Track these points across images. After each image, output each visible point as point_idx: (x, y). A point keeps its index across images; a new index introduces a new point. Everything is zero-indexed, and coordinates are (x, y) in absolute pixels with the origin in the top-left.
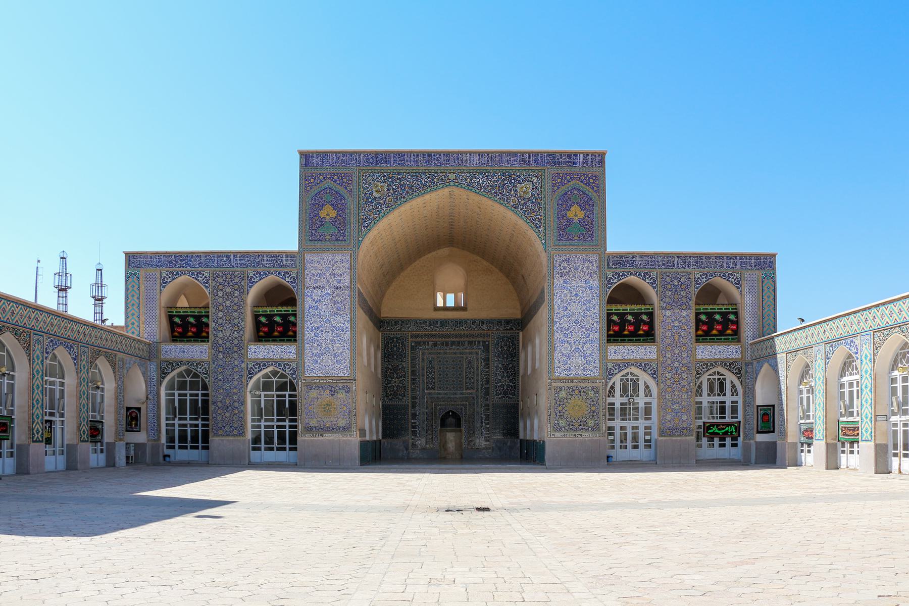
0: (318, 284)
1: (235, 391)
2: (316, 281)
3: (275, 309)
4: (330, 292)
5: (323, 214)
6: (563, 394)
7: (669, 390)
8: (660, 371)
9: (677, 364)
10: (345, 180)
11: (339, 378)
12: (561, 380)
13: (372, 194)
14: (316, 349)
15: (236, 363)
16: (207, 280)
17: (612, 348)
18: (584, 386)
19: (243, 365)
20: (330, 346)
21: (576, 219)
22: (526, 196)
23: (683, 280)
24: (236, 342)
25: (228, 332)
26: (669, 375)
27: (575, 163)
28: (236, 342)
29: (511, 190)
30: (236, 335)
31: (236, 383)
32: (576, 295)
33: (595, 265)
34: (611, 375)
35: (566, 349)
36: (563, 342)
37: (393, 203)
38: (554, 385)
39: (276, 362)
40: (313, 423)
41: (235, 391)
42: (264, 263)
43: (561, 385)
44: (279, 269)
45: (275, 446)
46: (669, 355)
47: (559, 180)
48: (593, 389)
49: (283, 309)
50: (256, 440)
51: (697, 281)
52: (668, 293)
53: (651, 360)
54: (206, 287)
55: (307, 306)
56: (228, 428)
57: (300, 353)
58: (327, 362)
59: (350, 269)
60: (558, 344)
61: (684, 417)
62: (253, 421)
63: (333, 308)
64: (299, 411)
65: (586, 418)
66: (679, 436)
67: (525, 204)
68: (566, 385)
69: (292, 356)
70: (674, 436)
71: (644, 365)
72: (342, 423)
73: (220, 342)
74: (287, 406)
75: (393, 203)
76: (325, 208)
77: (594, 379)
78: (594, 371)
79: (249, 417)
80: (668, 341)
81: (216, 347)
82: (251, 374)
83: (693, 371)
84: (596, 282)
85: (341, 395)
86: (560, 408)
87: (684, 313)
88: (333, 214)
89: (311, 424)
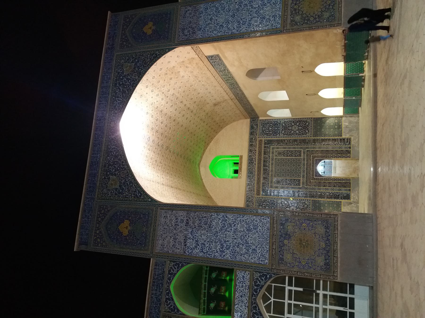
0: (182, 241)
5: (125, 232)
10: (103, 212)
12: (284, 21)
13: (116, 189)
14: (241, 249)
21: (153, 28)
29: (127, 79)
32: (211, 19)
33: (190, 8)
37: (125, 172)
38: (288, 27)
39: (254, 293)
40: (320, 261)
42: (158, 293)
43: (289, 21)
44: (166, 279)
47: (125, 43)
57: (245, 267)
58: (255, 239)
59: (173, 210)
63: (205, 229)
67: (138, 67)
72: (321, 230)
74: (301, 289)
75: (125, 172)
86: (312, 19)
88: (127, 223)
89: (322, 264)
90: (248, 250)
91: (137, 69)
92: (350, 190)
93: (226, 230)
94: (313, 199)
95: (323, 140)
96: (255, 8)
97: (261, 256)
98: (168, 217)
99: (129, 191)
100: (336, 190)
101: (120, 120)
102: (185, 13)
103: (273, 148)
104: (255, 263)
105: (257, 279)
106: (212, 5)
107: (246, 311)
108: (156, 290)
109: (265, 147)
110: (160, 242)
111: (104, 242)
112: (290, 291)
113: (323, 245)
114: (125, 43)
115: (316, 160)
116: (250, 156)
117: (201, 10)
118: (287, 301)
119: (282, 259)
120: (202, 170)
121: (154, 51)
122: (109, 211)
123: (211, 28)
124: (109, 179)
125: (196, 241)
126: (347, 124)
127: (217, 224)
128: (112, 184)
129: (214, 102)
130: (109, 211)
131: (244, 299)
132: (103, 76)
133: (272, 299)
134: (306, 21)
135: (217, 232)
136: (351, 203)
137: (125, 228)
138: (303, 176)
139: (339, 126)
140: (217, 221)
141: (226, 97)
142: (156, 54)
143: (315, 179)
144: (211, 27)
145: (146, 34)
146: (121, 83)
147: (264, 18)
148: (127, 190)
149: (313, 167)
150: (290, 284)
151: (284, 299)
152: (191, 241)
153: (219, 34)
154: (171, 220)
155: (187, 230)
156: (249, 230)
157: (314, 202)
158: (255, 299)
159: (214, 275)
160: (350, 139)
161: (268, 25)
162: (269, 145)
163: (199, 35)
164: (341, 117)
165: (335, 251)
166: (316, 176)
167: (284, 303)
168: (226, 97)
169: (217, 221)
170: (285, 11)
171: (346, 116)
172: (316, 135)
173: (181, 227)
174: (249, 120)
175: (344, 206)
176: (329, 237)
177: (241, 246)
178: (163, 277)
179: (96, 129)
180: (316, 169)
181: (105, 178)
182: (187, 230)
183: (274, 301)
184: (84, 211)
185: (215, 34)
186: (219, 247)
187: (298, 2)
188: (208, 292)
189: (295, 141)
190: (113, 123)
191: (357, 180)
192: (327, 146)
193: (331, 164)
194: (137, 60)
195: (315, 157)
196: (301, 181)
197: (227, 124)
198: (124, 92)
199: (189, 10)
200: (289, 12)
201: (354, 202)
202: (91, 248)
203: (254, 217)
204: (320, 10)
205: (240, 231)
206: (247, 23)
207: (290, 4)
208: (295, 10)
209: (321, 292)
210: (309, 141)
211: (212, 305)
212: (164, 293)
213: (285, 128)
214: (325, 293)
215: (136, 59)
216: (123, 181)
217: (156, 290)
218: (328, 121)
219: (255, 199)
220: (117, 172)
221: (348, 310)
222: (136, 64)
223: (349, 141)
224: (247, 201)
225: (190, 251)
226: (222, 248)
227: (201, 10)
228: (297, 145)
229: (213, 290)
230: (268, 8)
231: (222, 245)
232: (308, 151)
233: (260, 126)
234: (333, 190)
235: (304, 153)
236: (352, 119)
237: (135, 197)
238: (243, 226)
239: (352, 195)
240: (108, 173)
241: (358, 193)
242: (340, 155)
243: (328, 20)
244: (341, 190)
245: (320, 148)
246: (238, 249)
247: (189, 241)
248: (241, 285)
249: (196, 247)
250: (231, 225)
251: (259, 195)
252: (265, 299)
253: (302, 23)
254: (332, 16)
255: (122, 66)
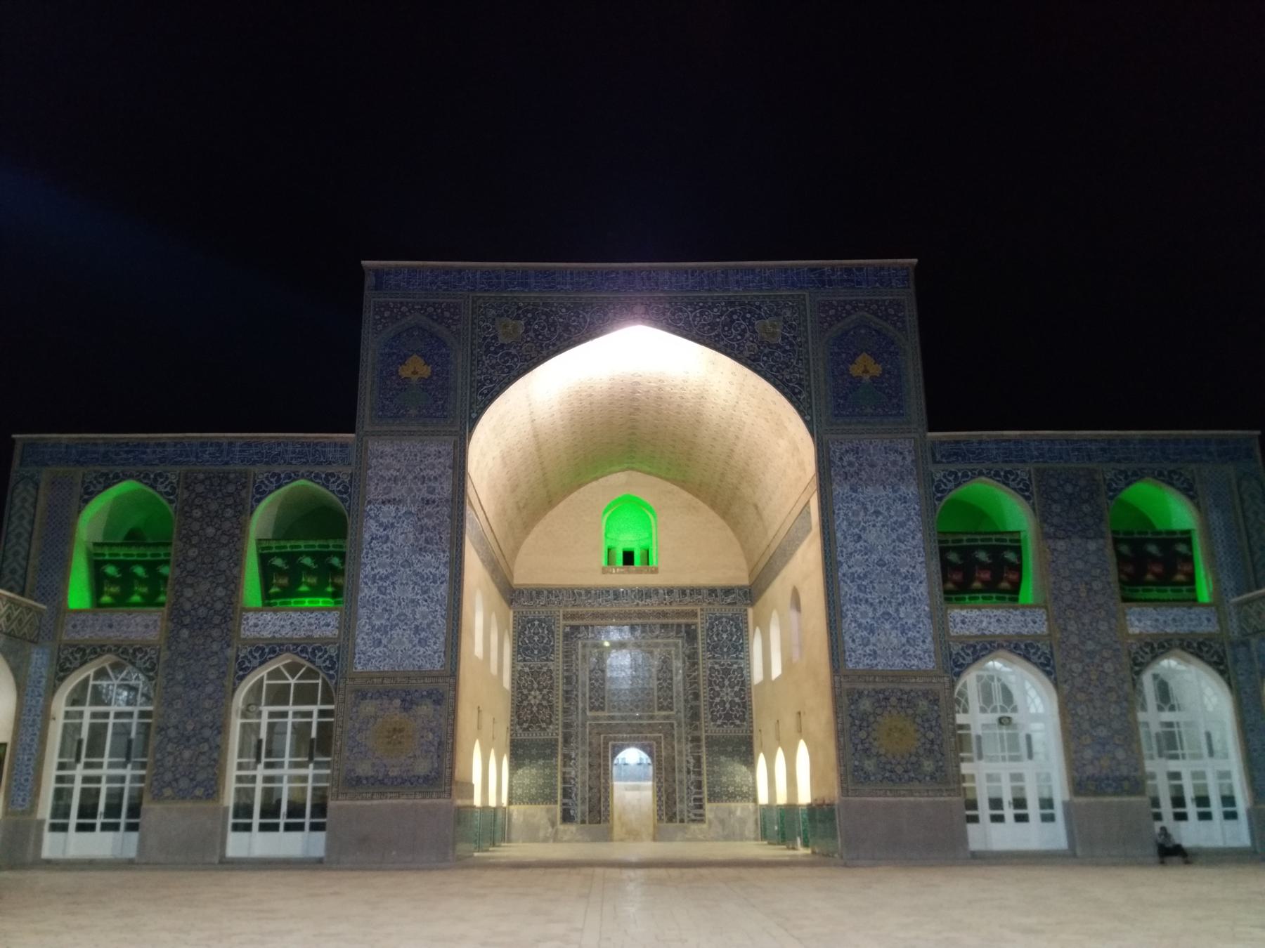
0: (392, 496)
1: (207, 704)
2: (388, 490)
3: (302, 545)
4: (413, 510)
5: (405, 372)
6: (866, 705)
7: (1081, 696)
8: (1058, 659)
9: (1090, 646)
10: (447, 314)
11: (422, 674)
13: (495, 338)
14: (380, 617)
15: (215, 647)
16: (174, 489)
17: (956, 613)
18: (907, 688)
19: (230, 652)
20: (408, 612)
21: (867, 378)
22: (773, 341)
23: (1082, 483)
24: (219, 606)
25: (204, 586)
26: (1077, 667)
27: (859, 283)
28: (219, 606)
29: (744, 331)
30: (220, 592)
31: (209, 689)
33: (909, 459)
34: (957, 667)
35: (864, 614)
36: (857, 601)
37: (533, 354)
38: (846, 686)
40: (364, 769)
41: (207, 704)
43: (861, 686)
44: (317, 469)
45: (282, 821)
46: (1072, 627)
47: (832, 312)
48: (925, 694)
49: (316, 545)
50: (243, 810)
51: (1109, 486)
52: (1056, 508)
53: (1038, 638)
54: (171, 502)
55: (367, 536)
56: (184, 783)
57: (348, 625)
58: (401, 642)
60: (848, 607)
61: (1120, 754)
62: (240, 766)
63: (417, 540)
64: (336, 744)
65: (917, 755)
66: (1115, 794)
67: (772, 353)
68: (871, 687)
69: (332, 632)
70: (1104, 794)
71: (1023, 649)
72: (423, 767)
73: (188, 606)
76: (409, 361)
77: (926, 674)
78: (923, 657)
79: (233, 758)
80: (1068, 599)
81: (177, 616)
82: (244, 669)
83: (1126, 660)
84: (913, 489)
85: (425, 709)
86: (863, 734)
87: (1092, 546)
88: (425, 371)
90: (378, 631)
91: (766, 351)
92: (583, 822)
93: (415, 583)
94: (560, 739)
95: (698, 760)
96: (897, 611)
97: (372, 655)
98: (442, 460)
99: (493, 367)
100: (580, 790)
101: (649, 325)
102: (896, 451)
103: (676, 645)
104: (355, 645)
105: (326, 652)
106: (913, 512)
107: (266, 634)
108: (294, 452)
109: (679, 625)
110: (388, 449)
111: (384, 327)
112: (309, 714)
113: (394, 772)
114: (832, 312)
115: (650, 746)
116: (656, 591)
117: (903, 488)
118: (291, 708)
119: (364, 697)
120: (620, 478)
121: (809, 386)
122: (449, 327)
123: (855, 514)
124: (518, 318)
125: (392, 524)
126: (738, 813)
127: (428, 565)
128: (506, 326)
129: (760, 505)
130: (449, 327)
131: (288, 628)
132: (752, 270)
133: (292, 681)
134: (857, 722)
135: (411, 565)
136: (553, 824)
137: (415, 368)
138: (612, 718)
139: (732, 797)
140: (434, 564)
141: (771, 534)
142: (800, 393)
143: (606, 744)
144: (858, 515)
145: (853, 362)
146: (735, 317)
147: (872, 631)
148: (494, 361)
149: (635, 739)
150: (322, 713)
151: (295, 703)
152: (393, 514)
153: (839, 535)
154: (433, 467)
155: (413, 502)
156: (417, 630)
157: (552, 745)
158: (288, 650)
159: (336, 561)
160: (702, 821)
161: (853, 641)
162: (683, 634)
163: (839, 489)
164: (755, 800)
165: (383, 795)
166: (614, 746)
167: (287, 703)
168: (771, 534)
169: (434, 564)
170: (884, 676)
171: (755, 812)
172: (712, 742)
173: (419, 490)
174: (745, 581)
175: (548, 811)
176: (408, 784)
177: (386, 616)
178: (320, 463)
179: (629, 273)
180: (628, 746)
181: (519, 308)
182: (413, 502)
183: (289, 685)
184: (447, 272)
185: (841, 524)
186: (382, 571)
187: (904, 704)
188: (301, 554)
189: (696, 696)
190: (639, 309)
191: (607, 837)
192: (685, 770)
193: (646, 779)
194: (788, 348)
195: (659, 743)
196: (600, 714)
197: (733, 530)
198: (713, 326)
199: (904, 458)
200: (882, 686)
201: (556, 832)
202: (371, 299)
203: (442, 639)
204: (882, 751)
205: (414, 613)
206: (862, 595)
207: (901, 686)
208: (887, 699)
209: (310, 771)
210: (696, 728)
211: (278, 562)
212: (289, 469)
213: (726, 672)
214: (310, 780)
215: (791, 345)
216: (513, 351)
217: (294, 452)
218: (744, 769)
219: (556, 609)
220: (532, 334)
221: (282, 821)
222: (778, 346)
223: (700, 819)
224: (550, 592)
225: (372, 513)
226: (381, 579)
227: (903, 488)
228: (686, 701)
229: (307, 561)
230: (895, 638)
231: (387, 577)
232: (672, 725)
233: (730, 611)
234: (584, 783)
235: (668, 717)
236: (750, 828)
237: (479, 381)
238: (424, 616)
239: (572, 828)
240: (530, 315)
241: (578, 841)
242: (664, 798)
243: (856, 769)
244: (583, 802)
245: (680, 753)
246: (379, 610)
247: (393, 508)
248: (313, 621)
249: (381, 525)
250: (425, 592)
251: (565, 617)
252: (293, 669)
253: (854, 714)
254: (867, 777)
255: (777, 315)
